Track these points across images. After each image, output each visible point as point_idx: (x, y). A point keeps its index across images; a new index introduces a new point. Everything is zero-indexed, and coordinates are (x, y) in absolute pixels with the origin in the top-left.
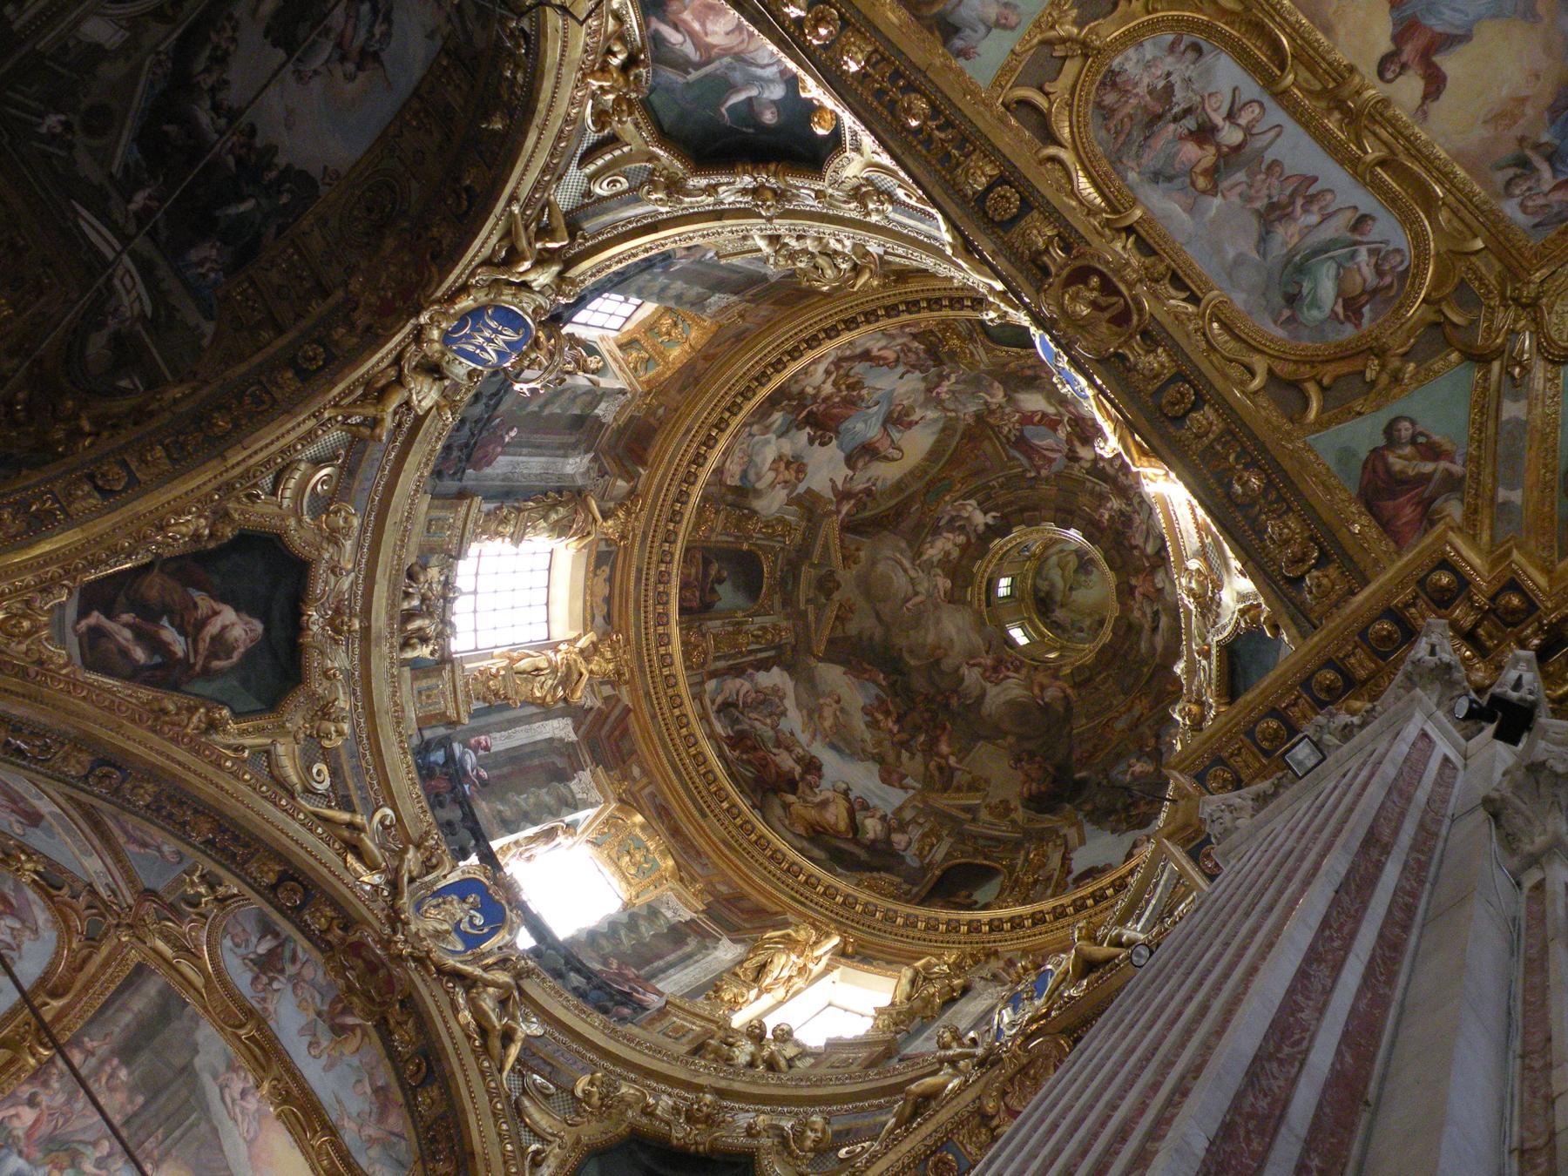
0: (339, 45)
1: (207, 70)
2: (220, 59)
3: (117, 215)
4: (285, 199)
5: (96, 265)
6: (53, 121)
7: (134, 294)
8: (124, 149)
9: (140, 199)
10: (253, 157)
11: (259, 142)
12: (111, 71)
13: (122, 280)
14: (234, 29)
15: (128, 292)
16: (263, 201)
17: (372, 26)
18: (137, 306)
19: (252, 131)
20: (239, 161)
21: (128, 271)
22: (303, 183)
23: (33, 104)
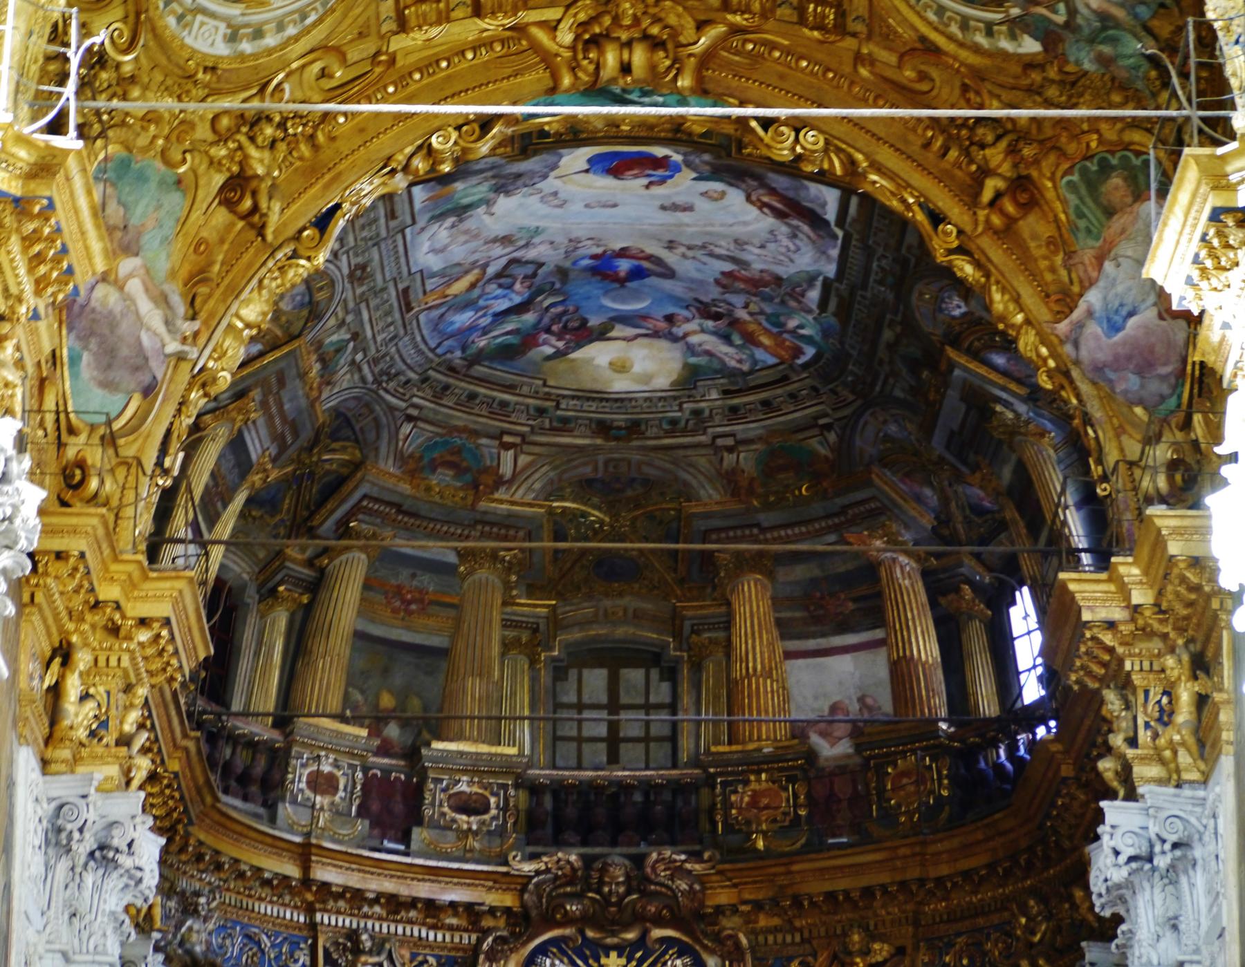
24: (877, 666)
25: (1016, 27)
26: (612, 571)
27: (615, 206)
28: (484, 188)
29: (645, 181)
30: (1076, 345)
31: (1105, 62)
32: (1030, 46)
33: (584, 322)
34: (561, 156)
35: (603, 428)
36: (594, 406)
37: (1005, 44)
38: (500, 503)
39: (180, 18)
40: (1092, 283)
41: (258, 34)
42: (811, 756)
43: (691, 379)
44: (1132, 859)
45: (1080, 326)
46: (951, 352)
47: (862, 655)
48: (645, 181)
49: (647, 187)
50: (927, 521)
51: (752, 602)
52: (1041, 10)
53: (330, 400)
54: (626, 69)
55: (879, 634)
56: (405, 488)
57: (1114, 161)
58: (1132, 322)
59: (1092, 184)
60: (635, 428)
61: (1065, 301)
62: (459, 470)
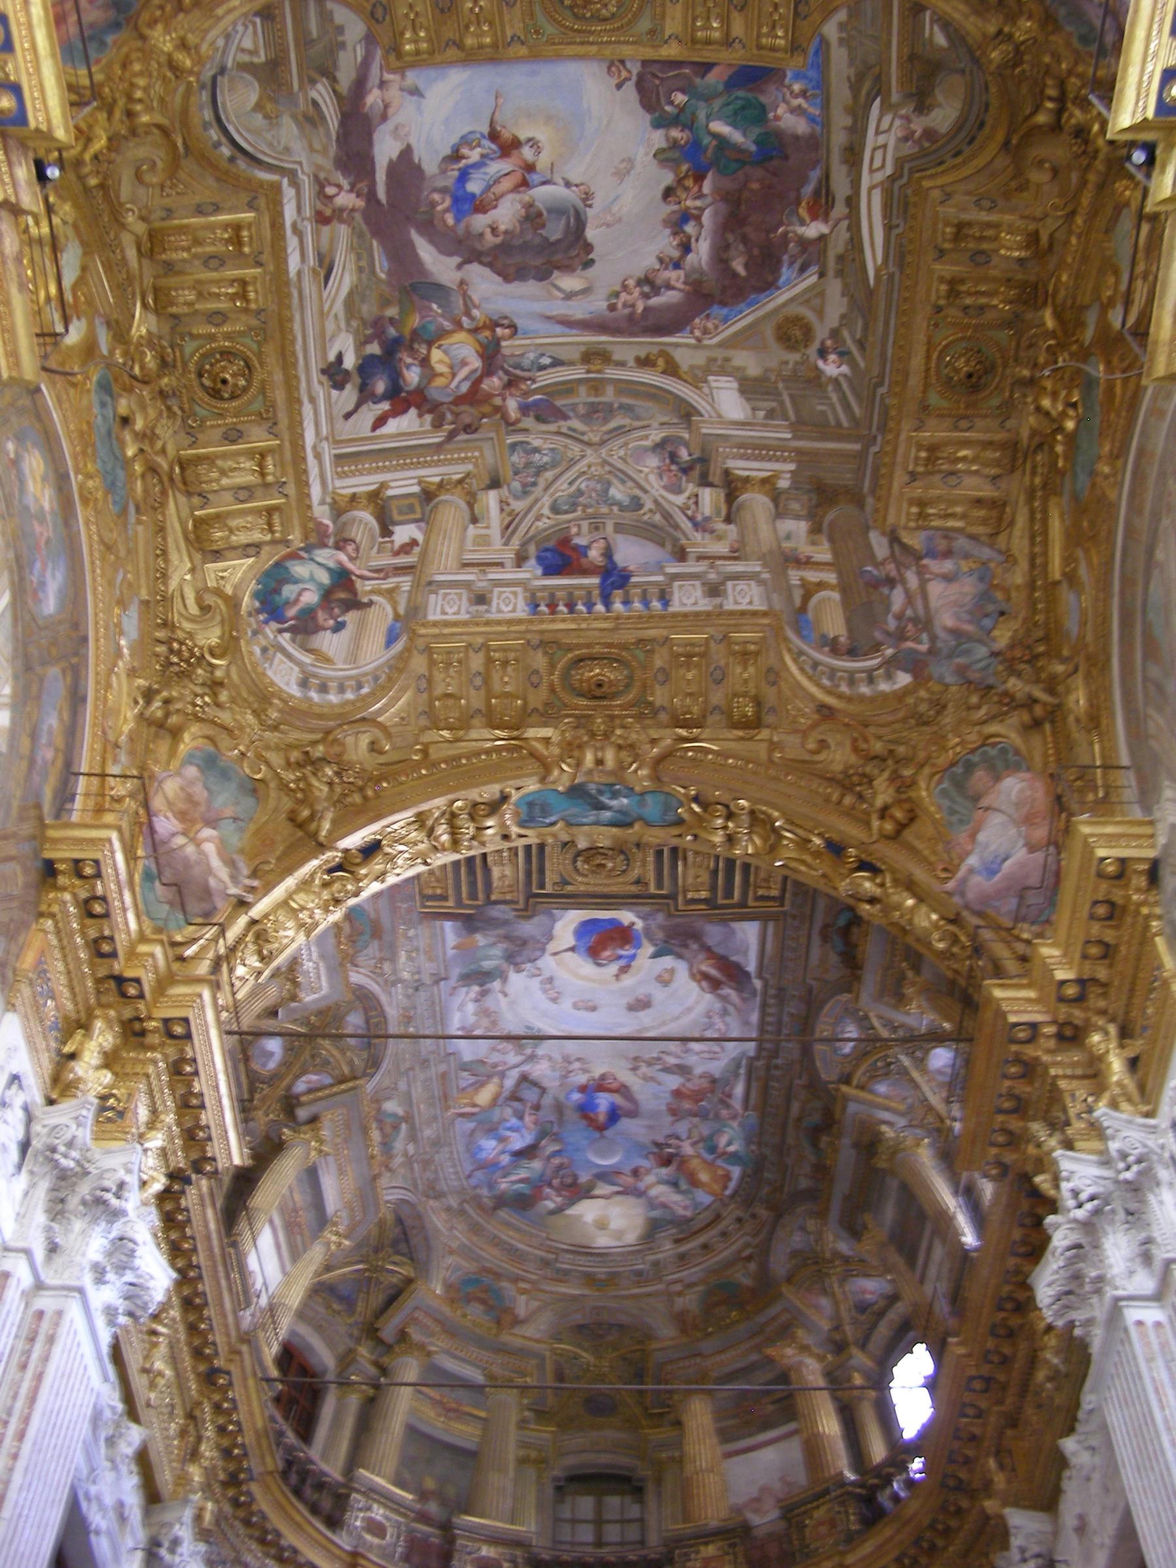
0: (524, 184)
1: (669, 287)
2: (650, 284)
3: (842, 235)
4: (680, 98)
5: (900, 202)
6: (831, 368)
7: (881, 139)
8: (792, 288)
9: (813, 230)
10: (685, 167)
11: (668, 178)
12: (749, 362)
13: (883, 166)
14: (617, 295)
15: (885, 146)
16: (702, 115)
17: (477, 166)
18: (885, 124)
19: (668, 193)
20: (699, 178)
21: (872, 171)
22: (650, 88)
23: (834, 397)
24: (793, 1450)
25: (891, 665)
26: (599, 1407)
27: (593, 1009)
28: (497, 951)
29: (614, 968)
30: (962, 894)
31: (961, 671)
32: (904, 679)
33: (575, 1177)
34: (554, 920)
35: (590, 1280)
36: (582, 1260)
37: (884, 687)
38: (513, 1338)
39: (264, 650)
40: (968, 853)
41: (323, 689)
42: (746, 1529)
43: (653, 1228)
44: (1092, 1198)
45: (964, 881)
46: (844, 1088)
47: (782, 1445)
48: (614, 968)
49: (617, 976)
50: (825, 1325)
51: (700, 1416)
52: (910, 644)
53: (391, 1191)
54: (600, 762)
55: (792, 1426)
56: (447, 1310)
57: (975, 758)
58: (1007, 863)
59: (959, 785)
60: (613, 1279)
61: (950, 870)
62: (490, 1308)
